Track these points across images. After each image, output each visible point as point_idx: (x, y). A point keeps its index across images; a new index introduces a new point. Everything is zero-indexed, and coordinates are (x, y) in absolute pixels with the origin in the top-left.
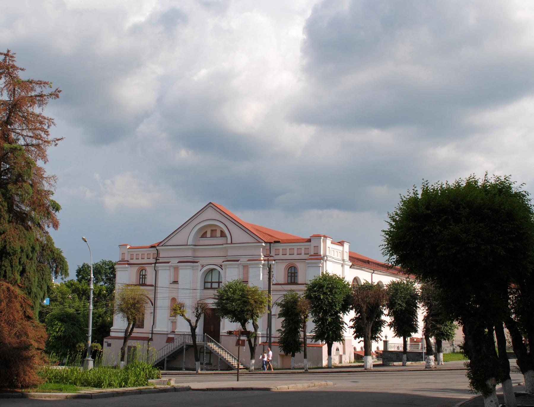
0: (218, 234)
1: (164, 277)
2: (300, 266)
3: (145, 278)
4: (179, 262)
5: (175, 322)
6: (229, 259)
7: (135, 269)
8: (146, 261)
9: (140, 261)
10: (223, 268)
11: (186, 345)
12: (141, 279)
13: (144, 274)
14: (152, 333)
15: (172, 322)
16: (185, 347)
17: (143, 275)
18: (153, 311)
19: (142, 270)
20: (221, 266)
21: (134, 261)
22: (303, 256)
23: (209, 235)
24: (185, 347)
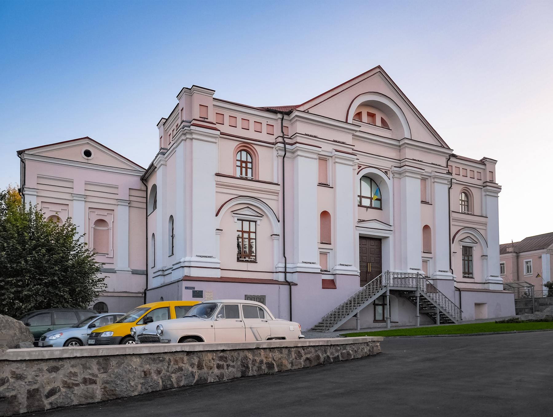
0: (378, 122)
1: (306, 169)
2: (476, 193)
3: (246, 168)
4: (337, 151)
5: (326, 254)
6: (407, 163)
10: (391, 175)
12: (239, 169)
13: (244, 159)
14: (285, 272)
15: (321, 253)
17: (242, 162)
18: (279, 231)
19: (241, 151)
20: (386, 173)
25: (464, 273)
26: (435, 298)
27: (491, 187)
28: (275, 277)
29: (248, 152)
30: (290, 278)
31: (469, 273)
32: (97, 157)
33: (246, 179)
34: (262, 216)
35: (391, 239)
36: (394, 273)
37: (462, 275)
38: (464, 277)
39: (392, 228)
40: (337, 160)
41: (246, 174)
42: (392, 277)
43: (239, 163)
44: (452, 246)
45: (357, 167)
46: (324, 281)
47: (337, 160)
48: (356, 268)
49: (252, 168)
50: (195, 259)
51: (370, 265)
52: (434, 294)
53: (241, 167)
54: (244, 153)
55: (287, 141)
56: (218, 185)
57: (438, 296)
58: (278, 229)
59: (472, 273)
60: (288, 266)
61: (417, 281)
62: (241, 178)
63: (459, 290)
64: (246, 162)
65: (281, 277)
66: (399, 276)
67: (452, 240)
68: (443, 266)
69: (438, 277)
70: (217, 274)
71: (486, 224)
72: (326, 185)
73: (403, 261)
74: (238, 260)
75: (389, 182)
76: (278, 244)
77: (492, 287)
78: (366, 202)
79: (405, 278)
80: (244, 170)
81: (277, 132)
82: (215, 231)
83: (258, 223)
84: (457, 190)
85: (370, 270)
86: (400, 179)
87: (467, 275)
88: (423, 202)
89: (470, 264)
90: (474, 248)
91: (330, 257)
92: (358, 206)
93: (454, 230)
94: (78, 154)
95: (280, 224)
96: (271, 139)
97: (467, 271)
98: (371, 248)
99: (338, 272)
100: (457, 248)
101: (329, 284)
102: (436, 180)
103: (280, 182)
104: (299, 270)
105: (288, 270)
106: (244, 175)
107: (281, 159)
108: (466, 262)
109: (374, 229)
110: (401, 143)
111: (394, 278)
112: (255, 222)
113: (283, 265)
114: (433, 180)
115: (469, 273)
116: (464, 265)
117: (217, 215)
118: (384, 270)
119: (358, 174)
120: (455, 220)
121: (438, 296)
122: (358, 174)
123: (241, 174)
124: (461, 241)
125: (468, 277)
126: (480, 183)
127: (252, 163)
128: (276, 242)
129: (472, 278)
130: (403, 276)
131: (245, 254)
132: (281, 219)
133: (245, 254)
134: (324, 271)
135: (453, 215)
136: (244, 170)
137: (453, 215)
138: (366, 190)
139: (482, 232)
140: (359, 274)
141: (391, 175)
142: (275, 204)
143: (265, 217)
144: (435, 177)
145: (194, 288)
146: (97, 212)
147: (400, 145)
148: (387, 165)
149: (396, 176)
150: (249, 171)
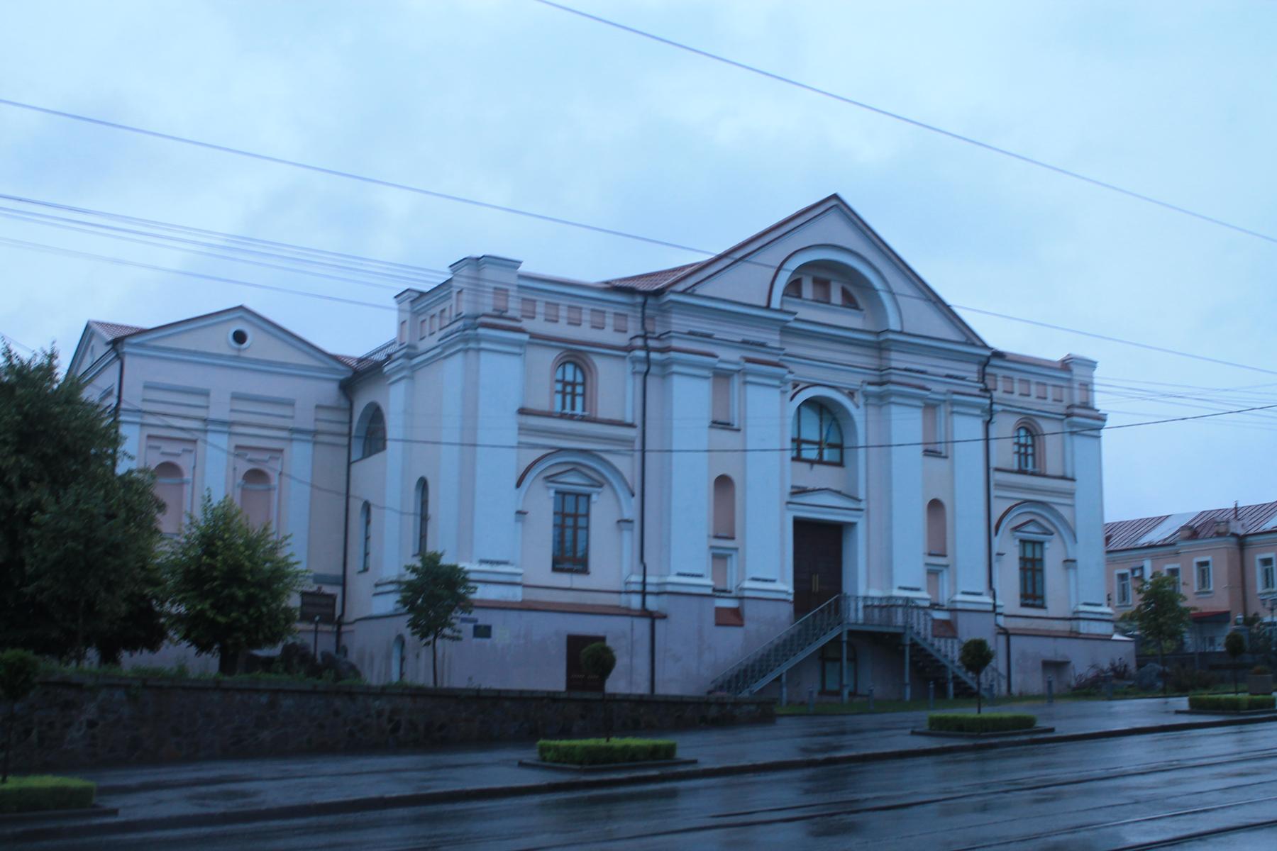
0: (836, 297)
1: (689, 398)
3: (574, 395)
4: (749, 360)
6: (894, 378)
7: (546, 358)
8: (585, 332)
9: (562, 329)
11: (851, 633)
12: (559, 397)
13: (569, 377)
14: (644, 593)
15: (715, 556)
16: (845, 638)
17: (565, 383)
19: (564, 364)
20: (851, 394)
21: (538, 325)
22: (1049, 405)
23: (808, 290)
24: (845, 638)
25: (1024, 596)
26: (943, 649)
27: (1084, 420)
28: (621, 600)
29: (576, 366)
30: (652, 603)
31: (1035, 597)
32: (257, 343)
33: (571, 417)
34: (601, 486)
35: (861, 530)
36: (865, 598)
37: (1018, 600)
38: (1023, 605)
39: (862, 505)
40: (749, 378)
41: (573, 407)
42: (861, 605)
43: (559, 387)
44: (995, 541)
45: (790, 387)
46: (719, 610)
47: (749, 378)
48: (786, 586)
49: (583, 395)
50: (476, 567)
51: (816, 578)
52: (943, 641)
53: (564, 393)
54: (570, 369)
55: (652, 343)
56: (522, 429)
57: (949, 644)
58: (630, 509)
59: (1042, 597)
60: (649, 579)
61: (905, 615)
62: (562, 416)
63: (1006, 633)
64: (573, 384)
65: (635, 602)
66: (876, 603)
67: (992, 529)
68: (976, 583)
69: (959, 606)
70: (516, 594)
71: (1071, 494)
72: (725, 425)
73: (886, 571)
74: (556, 569)
75: (857, 412)
76: (629, 540)
77: (1084, 627)
78: (811, 453)
79: (888, 605)
80: (568, 398)
81: (634, 327)
82: (513, 515)
83: (594, 498)
84: (1005, 426)
85: (816, 587)
86: (880, 406)
87: (1030, 602)
88: (929, 453)
89: (1038, 578)
90: (1047, 545)
91: (733, 564)
92: (793, 459)
93: (998, 508)
94: (220, 340)
95: (636, 501)
96: (622, 340)
97: (1030, 591)
98: (820, 546)
99: (747, 594)
100: (1009, 547)
101: (731, 618)
102: (955, 409)
103: (638, 422)
104: (669, 588)
105: (649, 589)
106: (568, 410)
107: (639, 379)
108: (1029, 574)
109: (824, 508)
110: (882, 338)
111: (866, 607)
112: (588, 496)
113: (640, 579)
114: (949, 409)
115: (1035, 597)
116: (1024, 580)
117: (518, 485)
118: (847, 589)
119: (792, 398)
120: (1000, 486)
121: (949, 644)
122: (792, 398)
123: (564, 407)
124: (1016, 529)
125: (1033, 606)
126: (1060, 408)
127: (583, 384)
128: (626, 535)
129: (1042, 607)
130: (884, 603)
131: (570, 557)
132: (637, 491)
133: (570, 557)
134: (719, 592)
135: (997, 477)
136: (568, 398)
137: (997, 477)
138: (811, 431)
139: (1064, 511)
140: (791, 598)
141: (860, 399)
142: (626, 465)
143: (606, 489)
144: (953, 403)
145: (475, 621)
146: (251, 455)
147: (880, 344)
148: (854, 380)
149: (871, 400)
150: (579, 400)
